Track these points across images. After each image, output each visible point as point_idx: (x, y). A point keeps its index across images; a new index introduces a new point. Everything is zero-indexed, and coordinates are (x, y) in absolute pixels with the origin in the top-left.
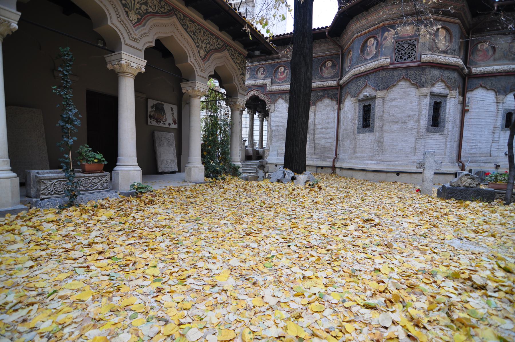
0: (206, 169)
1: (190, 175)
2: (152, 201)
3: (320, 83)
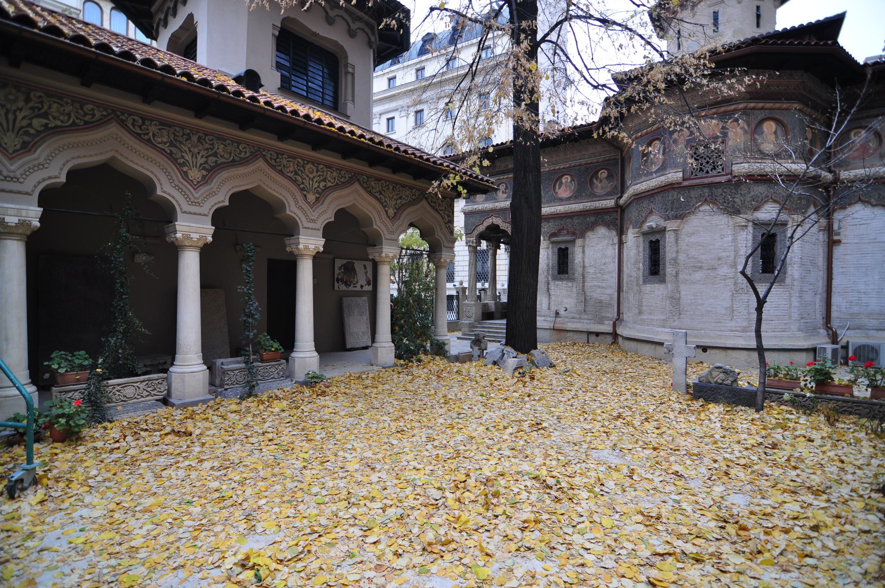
1: (376, 356)
2: (325, 392)
3: (589, 204)
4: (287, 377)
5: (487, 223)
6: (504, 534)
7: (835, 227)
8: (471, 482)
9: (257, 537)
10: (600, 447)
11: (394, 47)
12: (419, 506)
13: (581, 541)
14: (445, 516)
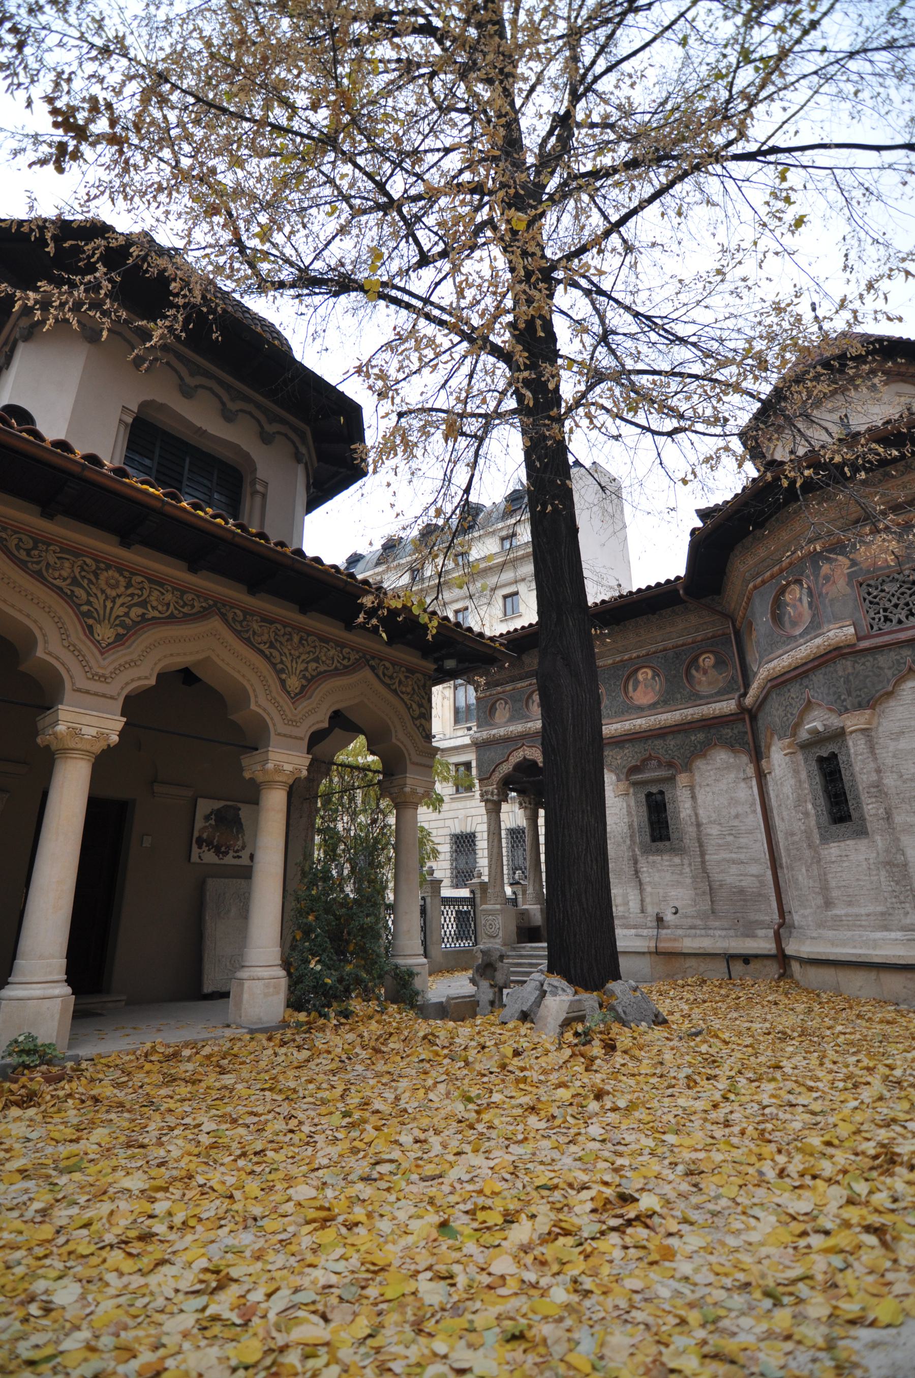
3: (691, 711)
5: (517, 757)
10: (883, 1310)
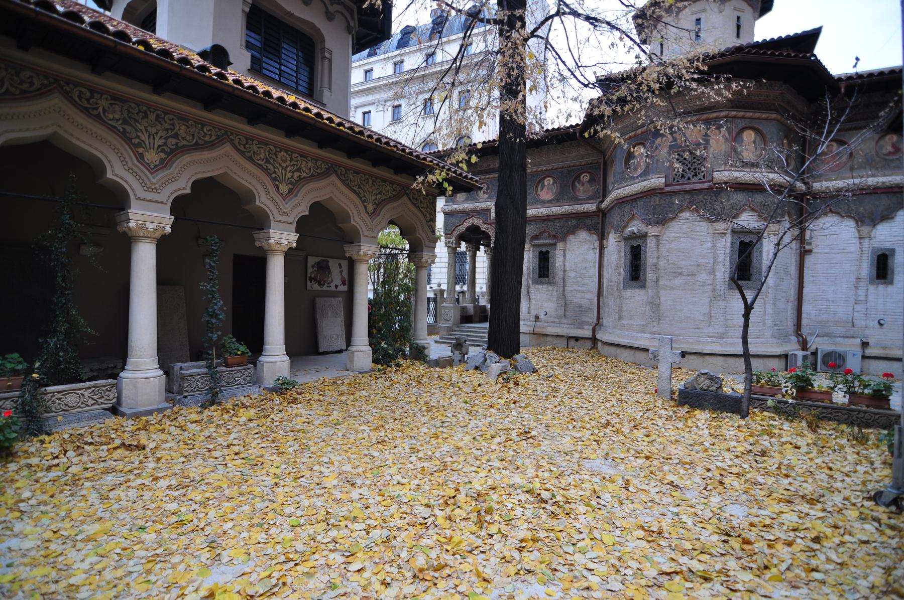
0: (375, 352)
1: (352, 360)
2: (297, 399)
3: (571, 207)
4: (255, 383)
5: (468, 223)
6: (501, 556)
7: (807, 237)
8: (461, 497)
9: (223, 568)
10: (592, 457)
11: (375, 34)
12: (407, 527)
13: (584, 561)
14: (436, 537)
